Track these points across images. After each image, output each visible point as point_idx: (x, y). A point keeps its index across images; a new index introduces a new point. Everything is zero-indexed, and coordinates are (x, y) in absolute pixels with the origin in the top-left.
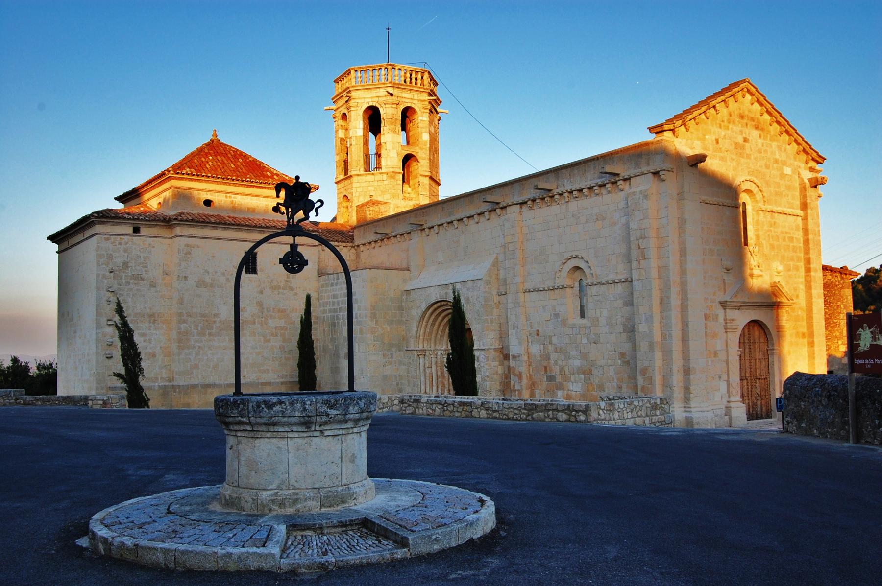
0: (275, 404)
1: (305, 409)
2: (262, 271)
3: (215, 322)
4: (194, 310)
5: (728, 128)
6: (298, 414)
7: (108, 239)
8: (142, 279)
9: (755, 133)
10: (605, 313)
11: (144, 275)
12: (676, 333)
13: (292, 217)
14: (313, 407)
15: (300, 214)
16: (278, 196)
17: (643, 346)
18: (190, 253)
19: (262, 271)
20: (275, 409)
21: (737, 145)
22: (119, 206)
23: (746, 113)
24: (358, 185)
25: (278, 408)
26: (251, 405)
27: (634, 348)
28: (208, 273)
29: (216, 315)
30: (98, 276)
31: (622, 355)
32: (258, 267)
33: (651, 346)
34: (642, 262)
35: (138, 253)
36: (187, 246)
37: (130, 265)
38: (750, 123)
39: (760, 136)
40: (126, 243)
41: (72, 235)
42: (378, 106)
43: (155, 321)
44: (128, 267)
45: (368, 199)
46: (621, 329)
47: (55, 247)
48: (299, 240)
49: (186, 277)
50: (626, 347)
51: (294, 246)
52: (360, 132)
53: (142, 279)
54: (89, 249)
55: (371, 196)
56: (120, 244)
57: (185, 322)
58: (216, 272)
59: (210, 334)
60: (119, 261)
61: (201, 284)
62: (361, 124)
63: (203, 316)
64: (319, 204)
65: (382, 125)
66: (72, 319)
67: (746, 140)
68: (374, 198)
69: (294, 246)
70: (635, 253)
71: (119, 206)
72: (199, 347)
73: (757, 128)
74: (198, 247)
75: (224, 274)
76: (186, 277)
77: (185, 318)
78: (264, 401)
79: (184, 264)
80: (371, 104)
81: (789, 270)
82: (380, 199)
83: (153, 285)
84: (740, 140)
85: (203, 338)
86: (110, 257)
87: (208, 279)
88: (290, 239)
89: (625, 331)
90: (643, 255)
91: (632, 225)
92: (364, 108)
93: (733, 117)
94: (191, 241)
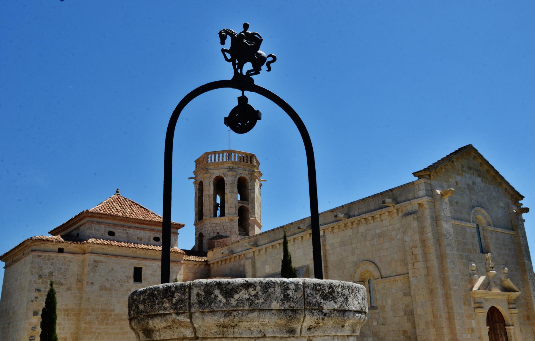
0: (236, 289)
1: (287, 298)
2: (145, 279)
3: (111, 315)
4: (97, 307)
5: (462, 175)
6: (275, 305)
7: (40, 256)
8: (62, 284)
9: (479, 180)
10: (390, 302)
11: (64, 282)
12: (444, 315)
13: (241, 67)
14: (299, 295)
15: (248, 66)
16: (223, 43)
17: (421, 325)
18: (96, 266)
19: (145, 279)
20: (236, 296)
21: (468, 185)
22: (50, 237)
23: (472, 166)
24: (209, 225)
25: (243, 295)
26: (195, 291)
27: (414, 326)
28: (108, 280)
29: (112, 310)
30: (30, 281)
31: (405, 332)
32: (143, 277)
33: (427, 324)
34: (415, 264)
35: (61, 266)
36: (95, 261)
37: (54, 274)
38: (475, 172)
39: (482, 181)
40: (53, 259)
41: (15, 255)
42: (223, 176)
43: (68, 314)
44: (52, 276)
45: (215, 234)
46: (402, 313)
47: (3, 264)
48: (247, 93)
49: (92, 283)
50: (407, 326)
51: (243, 100)
52: (212, 192)
53: (62, 284)
54: (26, 265)
55: (218, 233)
56: (49, 259)
57: (90, 315)
58: (114, 280)
59: (107, 324)
60: (46, 271)
61: (103, 288)
62: (212, 188)
63: (103, 310)
64: (270, 59)
65: (226, 187)
66: (8, 315)
67: (474, 183)
68: (220, 234)
69: (243, 100)
70: (409, 258)
71: (50, 237)
72: (99, 333)
73: (479, 176)
74: (102, 262)
75: (119, 282)
76: (92, 283)
77: (90, 312)
78: (219, 284)
79: (92, 274)
80: (218, 175)
81: (512, 271)
82: (224, 234)
83: (69, 289)
84: (470, 182)
85: (102, 327)
86: (41, 268)
87: (108, 285)
88: (238, 93)
89: (405, 314)
90: (416, 258)
91: (407, 239)
92: (214, 177)
93: (465, 168)
94: (98, 258)
